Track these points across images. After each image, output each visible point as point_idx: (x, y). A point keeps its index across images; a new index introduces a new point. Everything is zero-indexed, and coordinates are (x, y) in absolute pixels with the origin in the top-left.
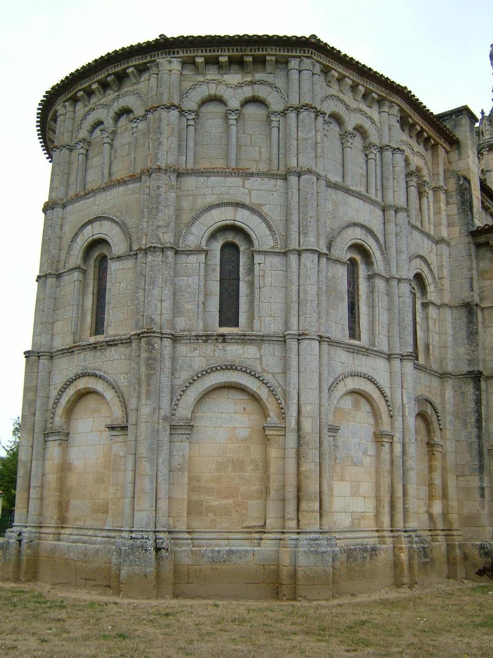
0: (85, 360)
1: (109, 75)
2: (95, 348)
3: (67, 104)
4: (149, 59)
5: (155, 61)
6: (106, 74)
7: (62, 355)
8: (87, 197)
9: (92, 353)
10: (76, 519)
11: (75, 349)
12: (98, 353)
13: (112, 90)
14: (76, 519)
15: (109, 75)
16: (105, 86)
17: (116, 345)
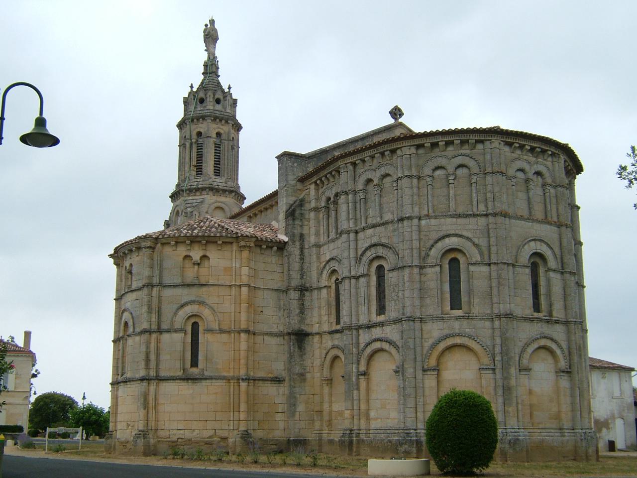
0: (542, 328)
1: (539, 148)
2: (548, 322)
3: (502, 143)
4: (557, 152)
5: (559, 155)
6: (539, 146)
7: (523, 321)
8: (527, 220)
9: (546, 324)
10: (539, 423)
11: (536, 320)
12: (550, 326)
13: (532, 155)
14: (539, 423)
15: (539, 148)
16: (532, 150)
17: (558, 323)
